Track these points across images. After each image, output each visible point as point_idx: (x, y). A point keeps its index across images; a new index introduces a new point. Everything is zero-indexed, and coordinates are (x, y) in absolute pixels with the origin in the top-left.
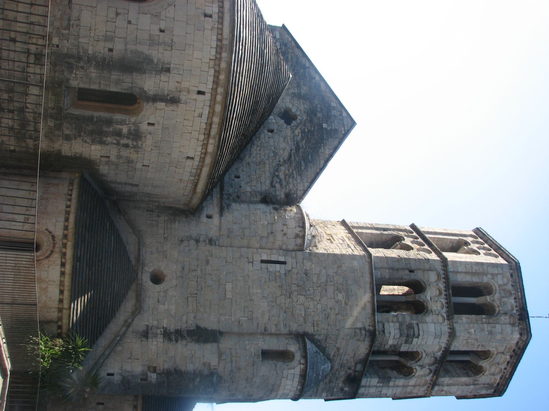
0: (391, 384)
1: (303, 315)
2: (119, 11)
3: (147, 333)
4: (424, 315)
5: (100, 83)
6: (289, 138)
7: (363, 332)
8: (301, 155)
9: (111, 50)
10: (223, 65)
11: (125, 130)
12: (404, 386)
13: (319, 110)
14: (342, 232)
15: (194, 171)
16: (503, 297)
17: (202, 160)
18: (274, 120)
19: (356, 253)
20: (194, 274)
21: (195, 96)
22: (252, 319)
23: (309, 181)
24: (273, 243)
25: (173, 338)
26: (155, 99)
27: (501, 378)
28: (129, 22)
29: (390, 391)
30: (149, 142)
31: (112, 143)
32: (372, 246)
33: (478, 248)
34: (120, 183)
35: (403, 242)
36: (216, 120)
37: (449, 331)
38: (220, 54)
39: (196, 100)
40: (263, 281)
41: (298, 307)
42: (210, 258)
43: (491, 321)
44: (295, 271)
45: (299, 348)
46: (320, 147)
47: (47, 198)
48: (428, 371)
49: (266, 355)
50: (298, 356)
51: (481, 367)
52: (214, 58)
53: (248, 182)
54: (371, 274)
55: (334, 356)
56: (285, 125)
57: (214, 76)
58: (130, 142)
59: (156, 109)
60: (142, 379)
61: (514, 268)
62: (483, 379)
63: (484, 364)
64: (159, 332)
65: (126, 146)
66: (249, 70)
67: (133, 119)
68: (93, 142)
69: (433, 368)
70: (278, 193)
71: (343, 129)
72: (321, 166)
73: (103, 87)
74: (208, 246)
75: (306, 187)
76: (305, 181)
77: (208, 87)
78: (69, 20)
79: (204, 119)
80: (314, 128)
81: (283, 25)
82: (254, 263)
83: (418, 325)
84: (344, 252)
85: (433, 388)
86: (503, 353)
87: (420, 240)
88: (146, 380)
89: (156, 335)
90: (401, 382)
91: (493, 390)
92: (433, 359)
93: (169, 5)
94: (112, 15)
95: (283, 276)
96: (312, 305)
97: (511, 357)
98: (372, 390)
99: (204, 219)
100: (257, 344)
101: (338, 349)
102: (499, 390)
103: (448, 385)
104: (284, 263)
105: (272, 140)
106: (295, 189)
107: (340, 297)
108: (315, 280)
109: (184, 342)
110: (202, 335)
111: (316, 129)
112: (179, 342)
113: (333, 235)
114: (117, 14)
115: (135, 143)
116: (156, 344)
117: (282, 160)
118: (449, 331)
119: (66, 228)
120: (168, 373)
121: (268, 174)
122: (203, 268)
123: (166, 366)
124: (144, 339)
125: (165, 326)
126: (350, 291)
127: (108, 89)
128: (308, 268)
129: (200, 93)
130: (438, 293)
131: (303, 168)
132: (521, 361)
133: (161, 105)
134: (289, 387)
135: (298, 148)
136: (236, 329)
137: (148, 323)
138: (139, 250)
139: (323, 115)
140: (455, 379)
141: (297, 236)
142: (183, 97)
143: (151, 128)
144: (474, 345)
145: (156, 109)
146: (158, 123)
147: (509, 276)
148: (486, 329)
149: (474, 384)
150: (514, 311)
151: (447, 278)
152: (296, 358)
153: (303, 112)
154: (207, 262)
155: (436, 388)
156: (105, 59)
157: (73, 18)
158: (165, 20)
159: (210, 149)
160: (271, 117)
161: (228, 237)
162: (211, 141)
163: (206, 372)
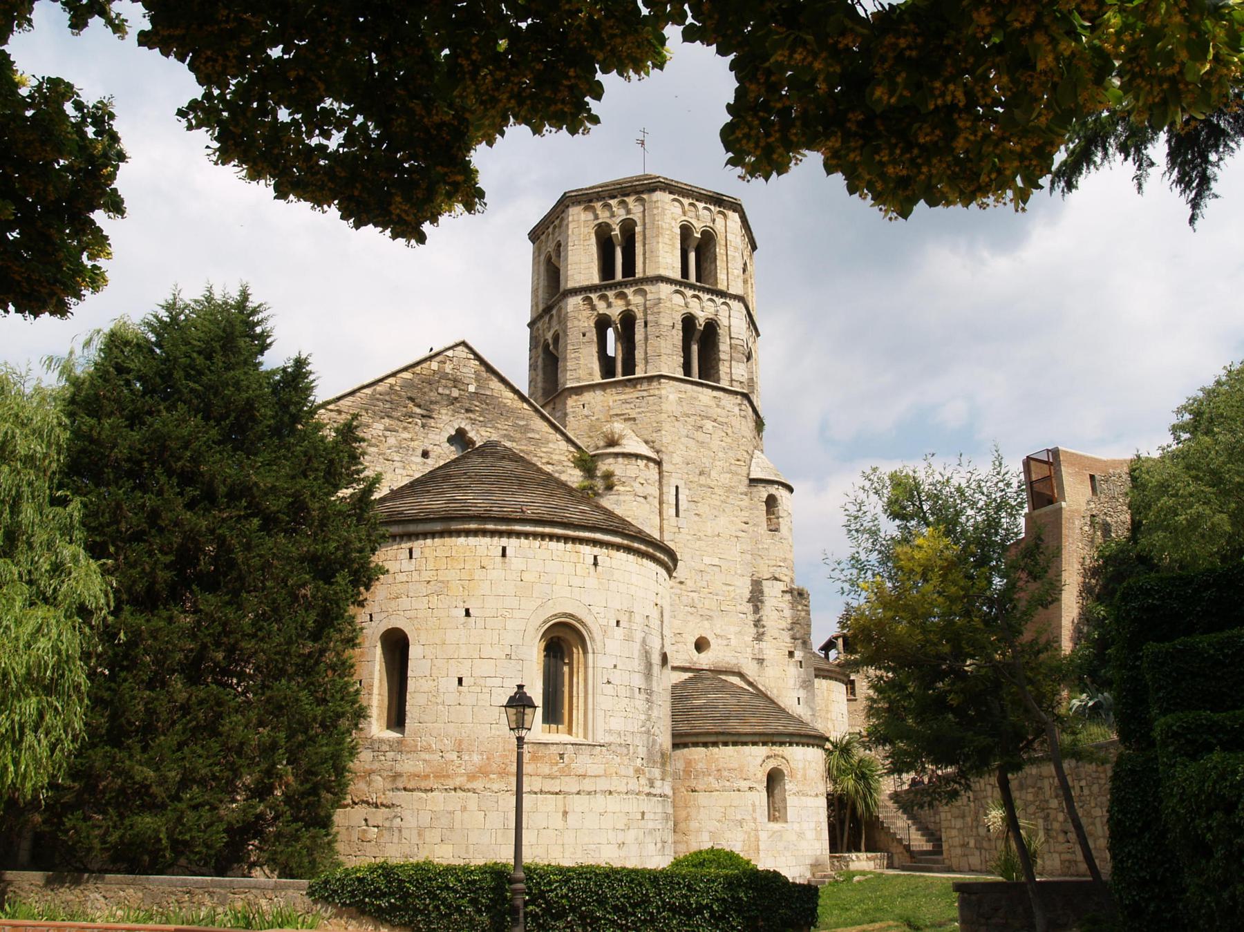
1: (729, 476)
8: (518, 435)
13: (447, 392)
25: (761, 630)
28: (615, 666)
40: (697, 518)
46: (505, 405)
50: (773, 490)
78: (620, 745)
89: (761, 650)
104: (677, 487)
109: (764, 618)
110: (756, 599)
119: (754, 744)
123: (788, 640)
131: (537, 436)
141: (646, 465)
150: (712, 207)
154: (681, 583)
157: (618, 741)
163: (788, 597)
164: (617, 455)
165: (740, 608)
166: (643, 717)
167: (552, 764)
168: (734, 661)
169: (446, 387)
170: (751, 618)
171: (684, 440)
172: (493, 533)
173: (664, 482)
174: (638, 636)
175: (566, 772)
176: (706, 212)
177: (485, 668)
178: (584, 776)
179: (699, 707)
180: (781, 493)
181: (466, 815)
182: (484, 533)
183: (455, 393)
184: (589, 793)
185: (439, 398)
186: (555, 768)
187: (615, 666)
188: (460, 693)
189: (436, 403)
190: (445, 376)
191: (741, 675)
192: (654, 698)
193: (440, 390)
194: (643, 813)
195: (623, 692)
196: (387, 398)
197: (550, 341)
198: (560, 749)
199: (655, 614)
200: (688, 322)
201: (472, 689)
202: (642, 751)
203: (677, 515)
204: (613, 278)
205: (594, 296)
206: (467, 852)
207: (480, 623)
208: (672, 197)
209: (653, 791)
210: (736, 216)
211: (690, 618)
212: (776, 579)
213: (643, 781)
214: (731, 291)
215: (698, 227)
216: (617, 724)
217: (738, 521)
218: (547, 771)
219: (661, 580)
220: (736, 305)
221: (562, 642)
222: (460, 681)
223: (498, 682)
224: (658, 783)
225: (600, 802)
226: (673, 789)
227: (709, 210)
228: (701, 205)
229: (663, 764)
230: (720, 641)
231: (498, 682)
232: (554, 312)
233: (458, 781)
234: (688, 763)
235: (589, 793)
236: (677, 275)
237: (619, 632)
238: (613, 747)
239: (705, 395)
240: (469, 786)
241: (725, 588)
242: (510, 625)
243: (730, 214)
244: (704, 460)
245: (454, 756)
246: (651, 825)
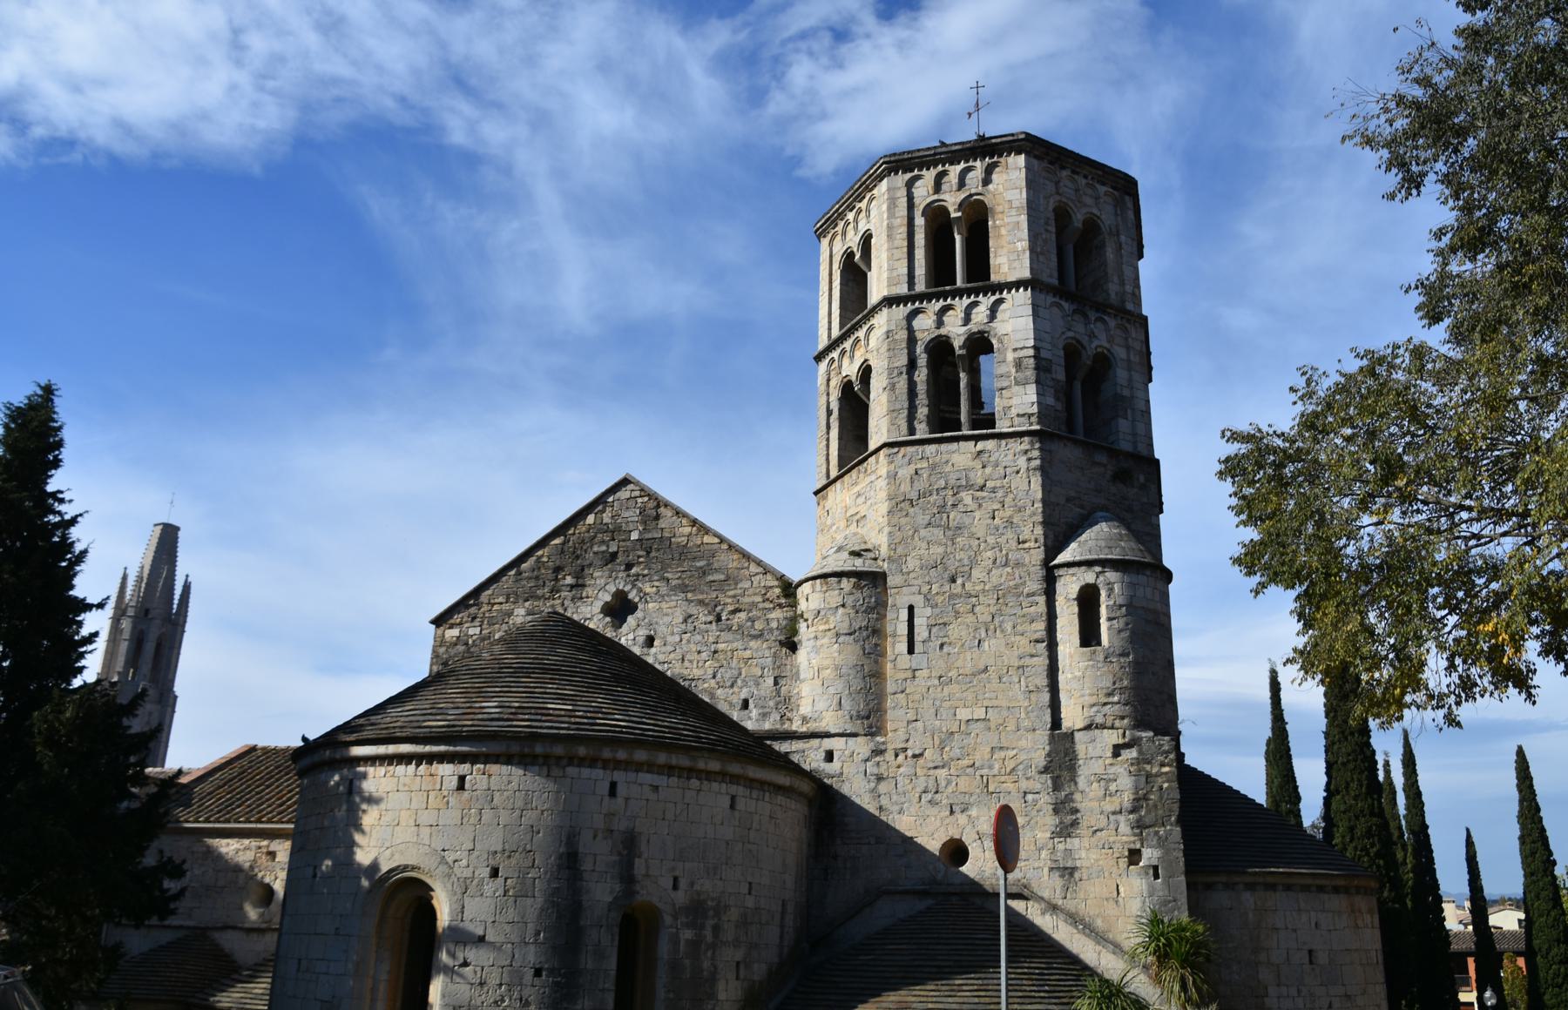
0: (1126, 392)
5: (603, 990)
6: (664, 605)
9: (538, 973)
10: (559, 750)
11: (687, 934)
12: (1129, 369)
14: (840, 496)
15: (755, 794)
17: (735, 779)
18: (629, 636)
19: (883, 471)
20: (943, 784)
21: (620, 800)
26: (627, 878)
27: (1103, 184)
29: (1140, 394)
30: (706, 885)
31: (713, 958)
32: (863, 438)
33: (856, 229)
34: (781, 937)
35: (854, 379)
36: (662, 758)
38: (535, 757)
39: (627, 799)
42: (910, 753)
43: (999, 209)
48: (1099, 324)
49: (1089, 636)
50: (1089, 576)
51: (1084, 223)
52: (545, 769)
53: (758, 684)
55: (1082, 507)
56: (639, 614)
57: (579, 766)
58: (710, 922)
59: (647, 875)
60: (1156, 876)
62: (1107, 217)
63: (1078, 218)
64: (1061, 847)
65: (716, 929)
66: (562, 698)
67: (668, 920)
68: (712, 995)
69: (1093, 315)
70: (774, 625)
73: (610, 984)
74: (889, 756)
75: (760, 570)
77: (599, 778)
79: (661, 780)
81: (433, 622)
83: (1015, 350)
84: (883, 495)
85: (1129, 312)
86: (1057, 183)
87: (847, 345)
88: (1156, 868)
89: (1068, 852)
90: (1121, 374)
91: (1127, 198)
92: (1076, 317)
95: (937, 611)
96: (989, 554)
97: (1063, 168)
98: (1140, 428)
99: (835, 767)
101: (1068, 500)
102: (1125, 187)
103: (1122, 283)
104: (911, 609)
105: (670, 639)
107: (967, 497)
108: (940, 550)
109: (1077, 796)
112: (1078, 806)
115: (711, 913)
116: (1084, 850)
117: (710, 618)
120: (1140, 826)
121: (739, 644)
123: (1124, 828)
124: (1077, 875)
127: (613, 973)
128: (918, 563)
129: (613, 792)
131: (722, 577)
132: (1069, 148)
133: (639, 866)
134: (1149, 590)
135: (684, 588)
136: (1046, 697)
137: (1046, 870)
138: (906, 892)
140: (1110, 271)
141: (856, 586)
142: (621, 825)
143: (683, 883)
144: (1045, 241)
145: (647, 875)
146: (673, 869)
147: (908, 176)
148: (1015, 219)
149: (1118, 235)
150: (978, 164)
151: (922, 297)
152: (1092, 581)
155: (1130, 306)
156: (556, 984)
159: (714, 766)
160: (623, 641)
161: (868, 718)
162: (701, 765)
165: (1024, 785)
169: (603, 542)
171: (923, 532)
183: (613, 548)
193: (596, 549)
200: (940, 347)
211: (935, 810)
212: (1103, 727)
214: (1012, 278)
215: (952, 200)
217: (1024, 641)
236: (920, 287)
237: (490, 887)
239: (960, 456)
244: (960, 555)
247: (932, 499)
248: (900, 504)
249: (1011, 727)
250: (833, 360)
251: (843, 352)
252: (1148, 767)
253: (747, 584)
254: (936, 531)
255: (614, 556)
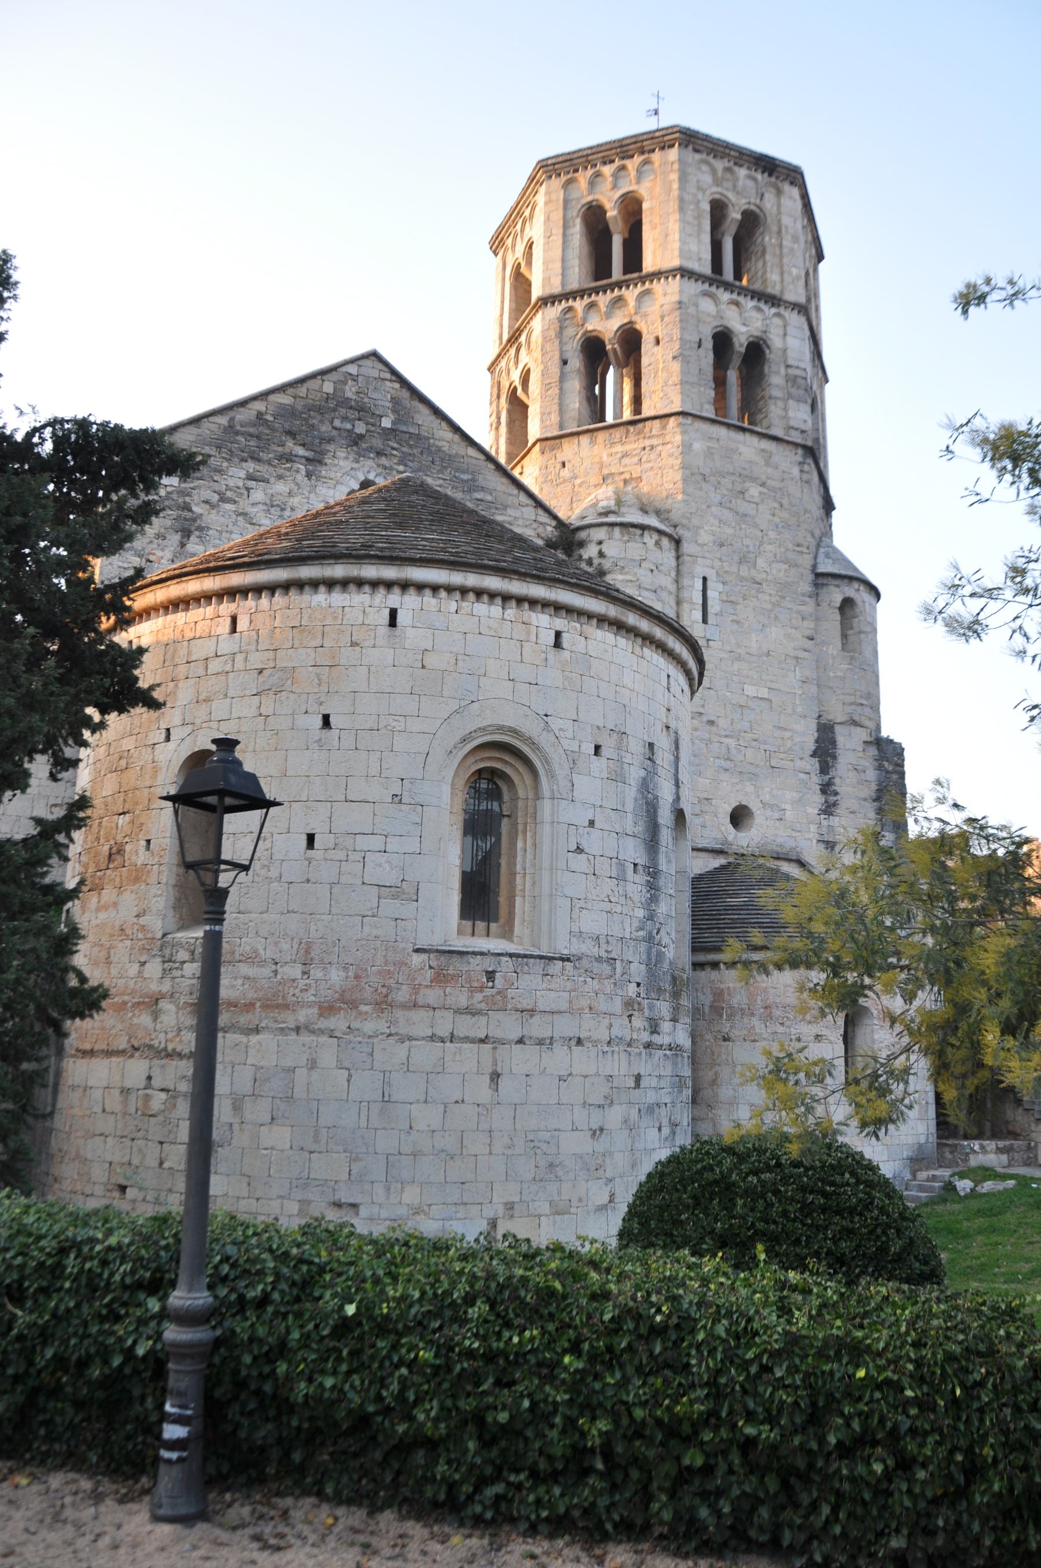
2: (574, 847)
3: (827, 843)
4: (768, 347)
7: (806, 468)
13: (349, 426)
16: (734, 186)
20: (734, 751)
22: (797, 658)
23: (516, 492)
24: (670, 593)
25: (832, 799)
28: (592, 823)
37: (796, 312)
41: (774, 572)
42: (705, 719)
43: (774, 229)
44: (717, 563)
45: (837, 586)
46: (439, 449)
47: (766, 1008)
50: (850, 591)
54: (713, 421)
61: (690, 139)
64: (825, 823)
71: (388, 384)
72: (482, 457)
75: (530, 502)
76: (516, 501)
78: (599, 959)
80: (393, 448)
82: (708, 636)
83: (788, 366)
93: (547, 726)
94: (580, 862)
95: (727, 588)
96: (769, 547)
100: (833, 658)
104: (705, 579)
106: (535, 525)
107: (754, 491)
109: (837, 781)
110: (825, 751)
111: (396, 445)
113: (606, 471)
114: (579, 850)
118: (796, 312)
122: (723, 733)
123: (872, 815)
124: (837, 849)
125: (816, 811)
126: (744, 472)
128: (711, 538)
130: (734, 307)
131: (489, 498)
139: (359, 419)
141: (657, 544)
153: (355, 465)
154: (711, 723)
158: (580, 741)
164: (612, 525)
166: (640, 913)
167: (472, 990)
168: (790, 844)
169: (345, 419)
170: (816, 780)
172: (375, 584)
173: (684, 569)
174: (635, 774)
175: (499, 1004)
176: (750, 183)
177: (355, 818)
178: (532, 1012)
179: (733, 908)
180: (862, 596)
181: (315, 1075)
182: (360, 583)
183: (360, 428)
184: (540, 1042)
185: (335, 433)
186: (479, 996)
187: (592, 823)
188: (310, 861)
189: (330, 440)
190: (345, 403)
191: (801, 864)
192: (662, 882)
193: (337, 423)
194: (638, 1078)
195: (605, 868)
196: (252, 430)
197: (517, 383)
198: (489, 964)
199: (663, 743)
200: (722, 340)
201: (331, 854)
202: (638, 971)
203: (705, 621)
204: (610, 276)
205: (579, 305)
206: (316, 1139)
207: (348, 741)
208: (698, 156)
209: (657, 1039)
210: (795, 192)
211: (724, 776)
213: (638, 1022)
216: (593, 922)
218: (463, 1001)
219: (675, 689)
220: (795, 319)
221: (496, 782)
222: (311, 839)
223: (377, 842)
224: (666, 1026)
225: (559, 1059)
226: (693, 1036)
227: (755, 180)
228: (742, 172)
229: (676, 995)
230: (769, 813)
231: (377, 842)
232: (523, 339)
233: (303, 1015)
234: (718, 995)
235: (540, 1042)
236: (707, 269)
237: (598, 765)
238: (585, 962)
239: (748, 447)
240: (323, 1024)
241: (778, 733)
242: (401, 743)
243: (786, 187)
245: (296, 971)
246: (651, 1097)
247: (723, 481)
248: (694, 476)
249: (790, 711)
250: (570, 309)
251: (592, 305)
252: (886, 764)
253: (517, 514)
254: (726, 512)
255: (361, 437)
